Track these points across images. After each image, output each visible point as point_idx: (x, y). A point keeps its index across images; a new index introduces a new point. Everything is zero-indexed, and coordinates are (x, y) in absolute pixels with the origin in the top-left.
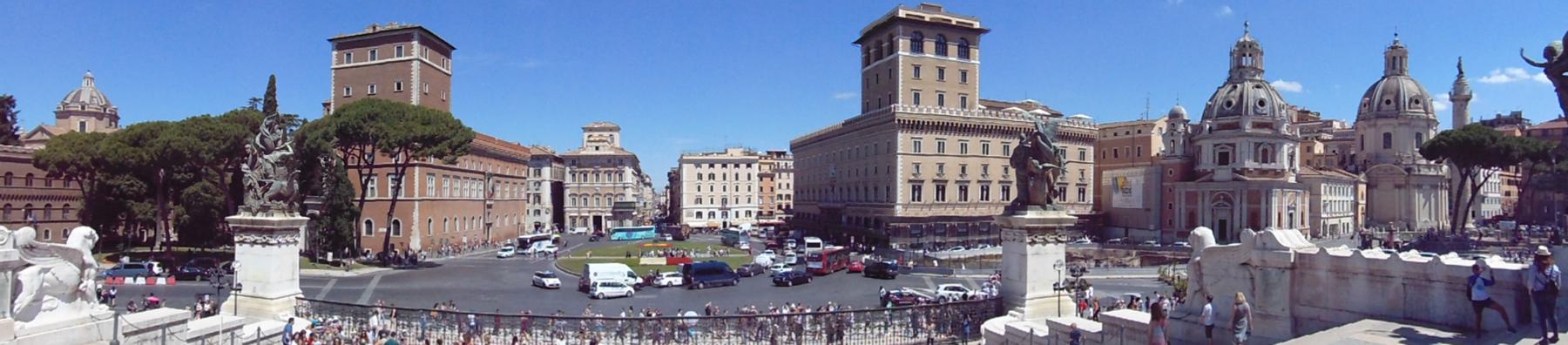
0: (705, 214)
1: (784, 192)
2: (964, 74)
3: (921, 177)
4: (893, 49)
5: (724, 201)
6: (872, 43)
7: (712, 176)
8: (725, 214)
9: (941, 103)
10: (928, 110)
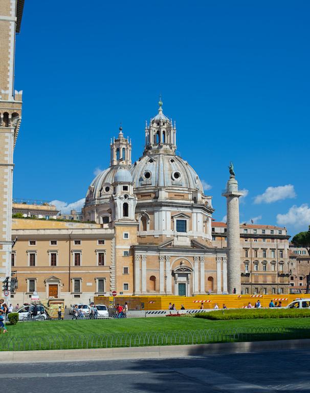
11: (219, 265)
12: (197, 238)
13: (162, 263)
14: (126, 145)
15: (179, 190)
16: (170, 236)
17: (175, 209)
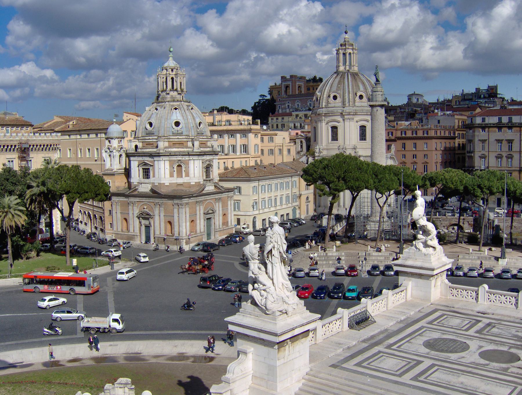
11: (176, 211)
12: (157, 184)
13: (130, 207)
14: (353, 49)
15: (149, 139)
16: (136, 184)
17: (140, 159)
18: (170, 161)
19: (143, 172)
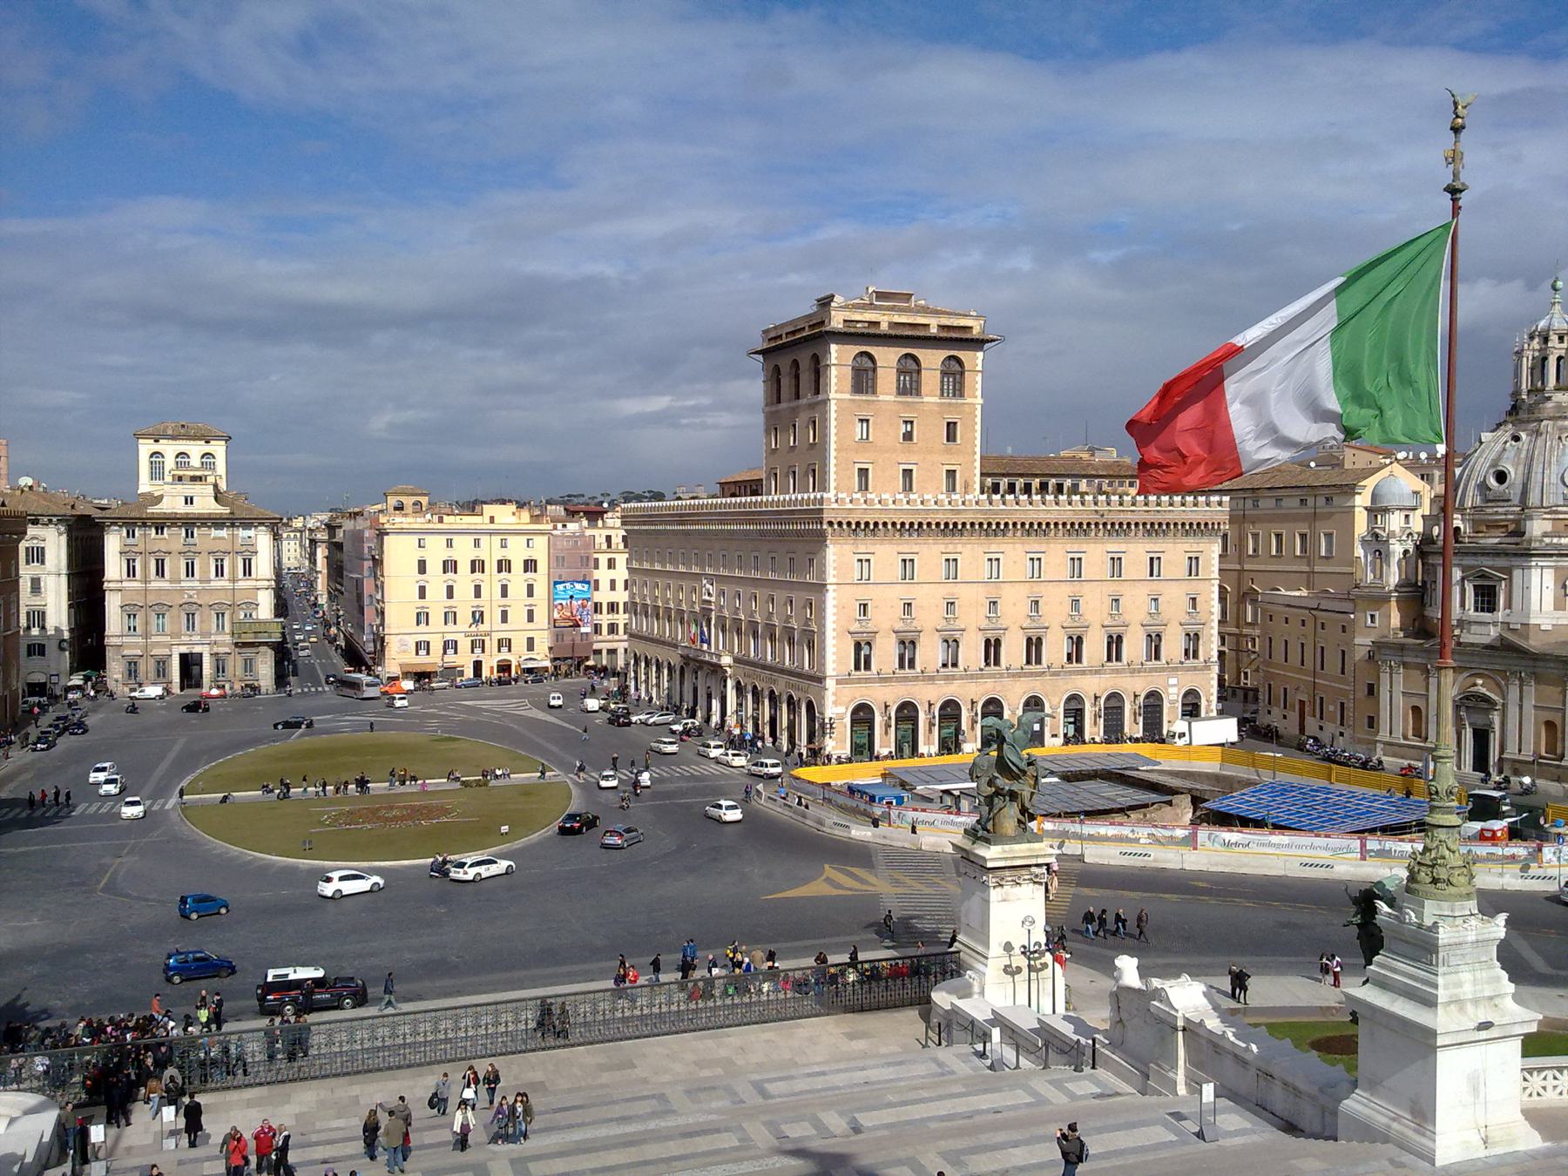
0: (437, 647)
1: (604, 596)
2: (951, 426)
3: (871, 627)
4: (818, 384)
5: (478, 617)
6: (785, 363)
7: (450, 566)
8: (478, 644)
9: (908, 487)
10: (886, 498)
18: (1556, 568)
19: (1476, 595)
